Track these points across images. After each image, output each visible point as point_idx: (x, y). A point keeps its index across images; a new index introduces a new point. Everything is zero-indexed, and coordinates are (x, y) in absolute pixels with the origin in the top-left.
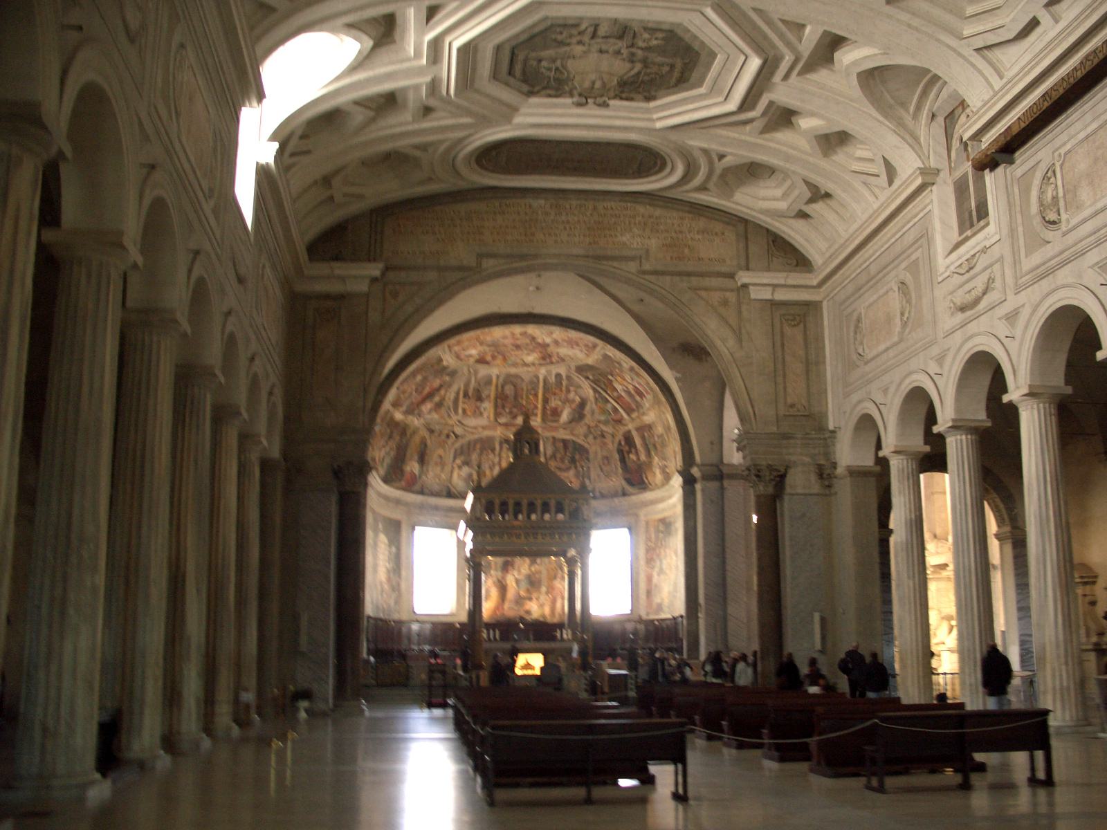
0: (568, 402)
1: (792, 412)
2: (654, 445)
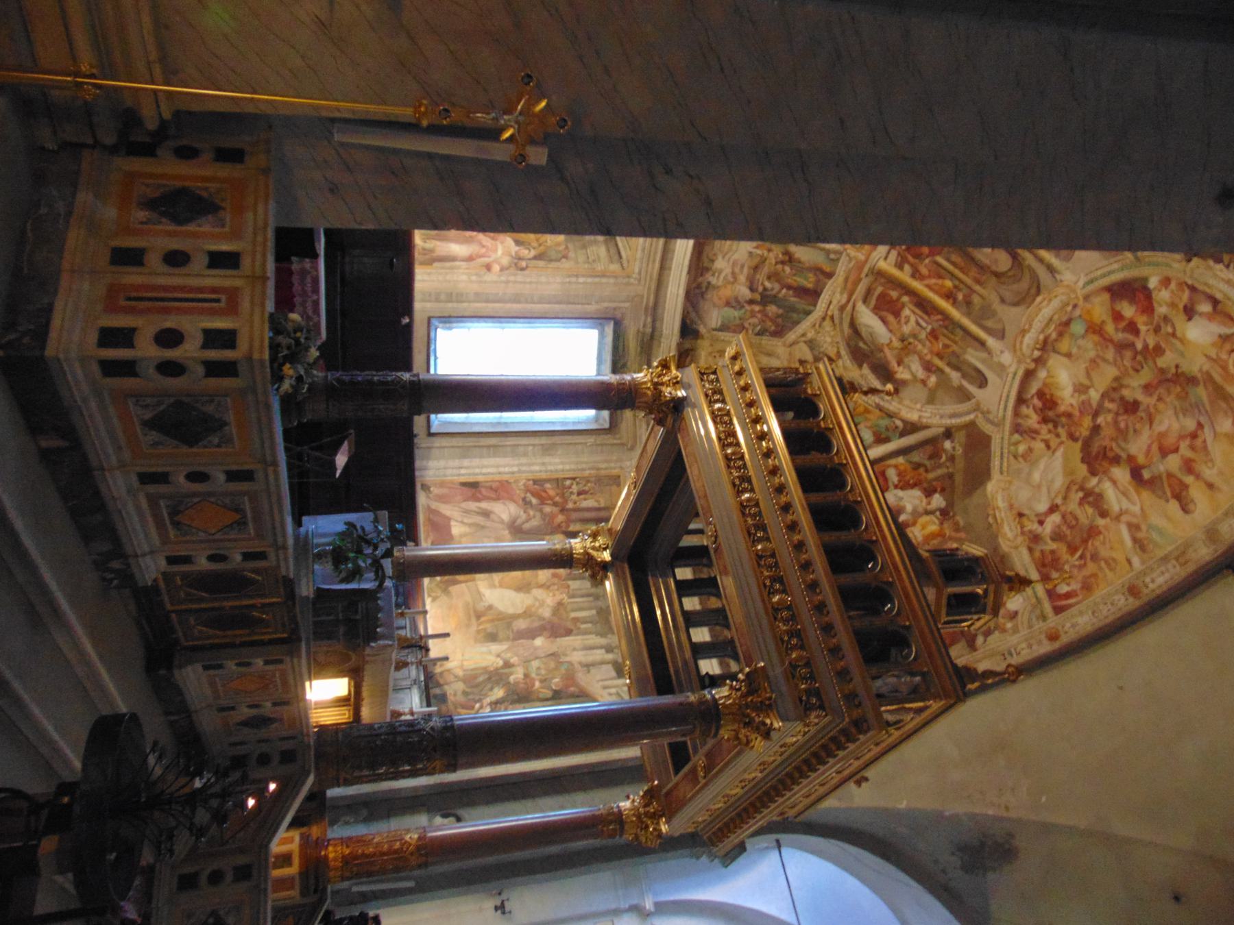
0: (902, 349)
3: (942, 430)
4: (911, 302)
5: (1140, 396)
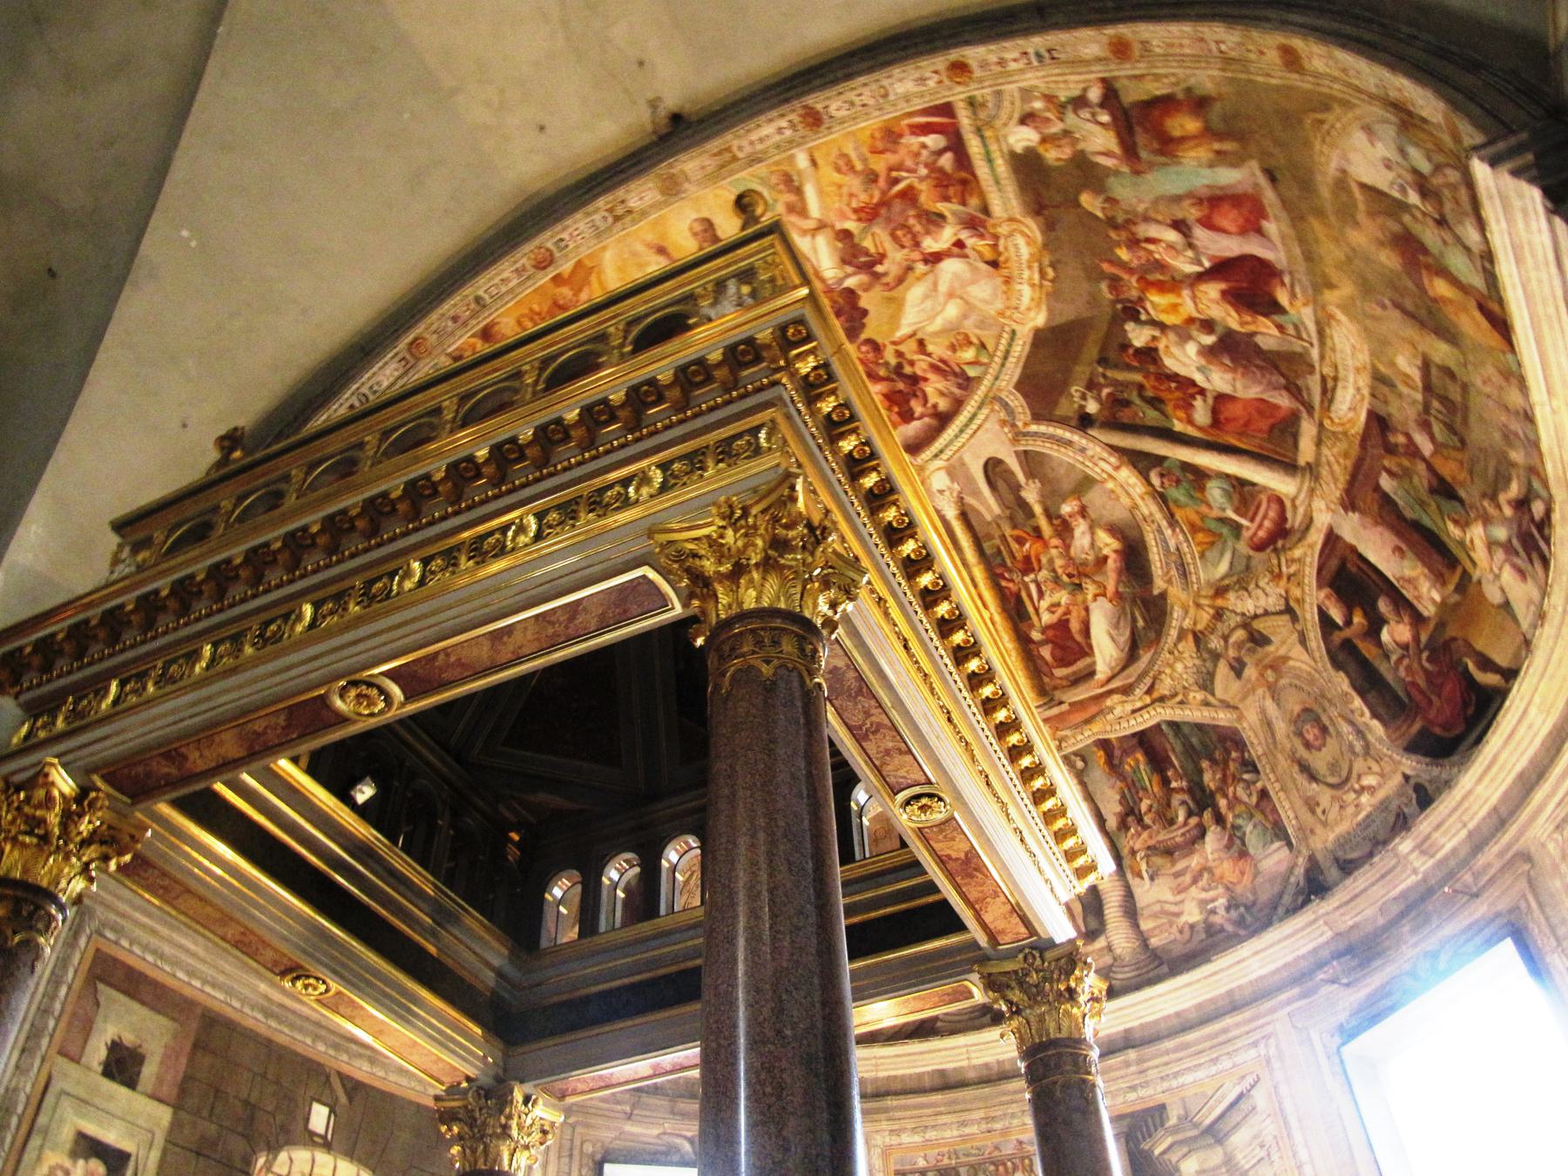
0: (1087, 576)
2: (1444, 490)
4: (1032, 626)
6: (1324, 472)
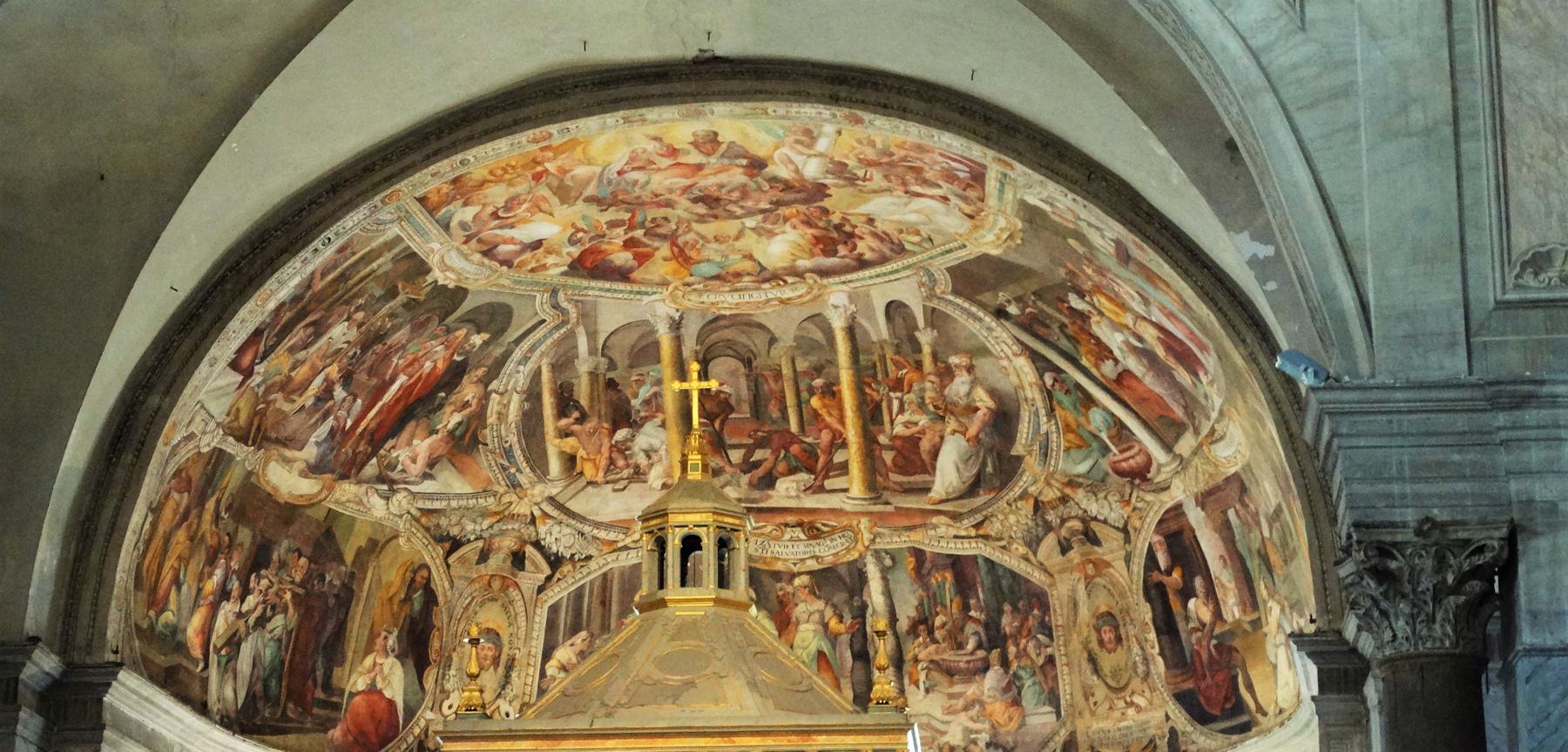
0: (952, 413)
1: (1535, 287)
3: (1007, 324)
4: (883, 431)
5: (684, 202)
6: (1191, 470)
